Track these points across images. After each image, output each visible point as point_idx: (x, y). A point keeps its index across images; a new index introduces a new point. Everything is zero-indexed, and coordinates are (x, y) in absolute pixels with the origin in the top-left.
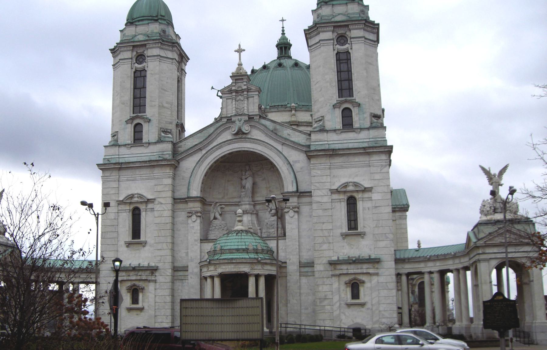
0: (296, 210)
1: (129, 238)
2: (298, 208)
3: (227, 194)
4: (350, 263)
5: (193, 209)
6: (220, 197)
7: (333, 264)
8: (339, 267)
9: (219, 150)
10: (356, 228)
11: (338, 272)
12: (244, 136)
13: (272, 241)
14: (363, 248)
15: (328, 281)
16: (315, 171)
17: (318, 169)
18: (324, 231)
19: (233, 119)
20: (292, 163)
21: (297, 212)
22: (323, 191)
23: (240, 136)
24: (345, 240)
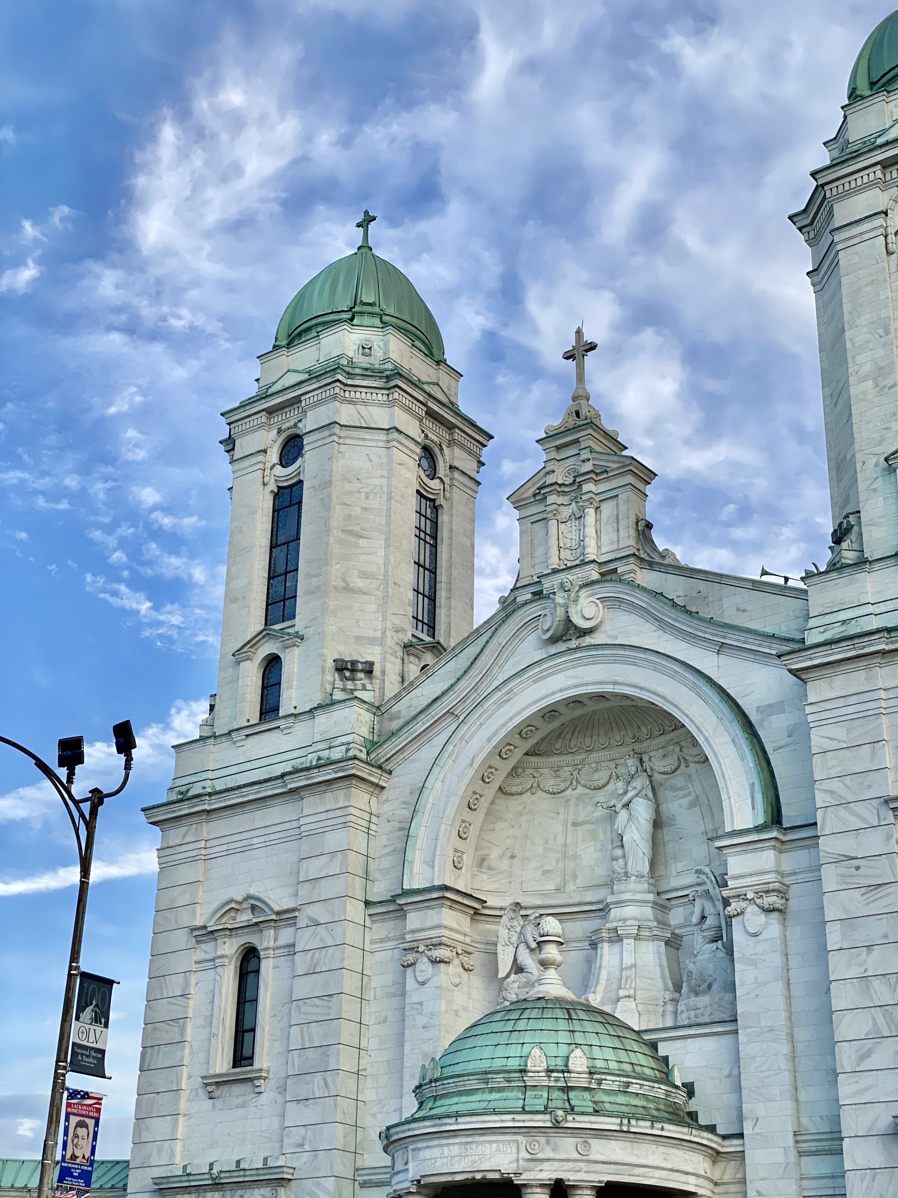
2: (782, 893)
3: (574, 876)
5: (422, 935)
6: (551, 886)
9: (507, 706)
12: (588, 640)
13: (692, 1045)
16: (823, 731)
17: (838, 721)
18: (876, 983)
19: (547, 584)
20: (754, 717)
22: (858, 808)
23: (573, 644)
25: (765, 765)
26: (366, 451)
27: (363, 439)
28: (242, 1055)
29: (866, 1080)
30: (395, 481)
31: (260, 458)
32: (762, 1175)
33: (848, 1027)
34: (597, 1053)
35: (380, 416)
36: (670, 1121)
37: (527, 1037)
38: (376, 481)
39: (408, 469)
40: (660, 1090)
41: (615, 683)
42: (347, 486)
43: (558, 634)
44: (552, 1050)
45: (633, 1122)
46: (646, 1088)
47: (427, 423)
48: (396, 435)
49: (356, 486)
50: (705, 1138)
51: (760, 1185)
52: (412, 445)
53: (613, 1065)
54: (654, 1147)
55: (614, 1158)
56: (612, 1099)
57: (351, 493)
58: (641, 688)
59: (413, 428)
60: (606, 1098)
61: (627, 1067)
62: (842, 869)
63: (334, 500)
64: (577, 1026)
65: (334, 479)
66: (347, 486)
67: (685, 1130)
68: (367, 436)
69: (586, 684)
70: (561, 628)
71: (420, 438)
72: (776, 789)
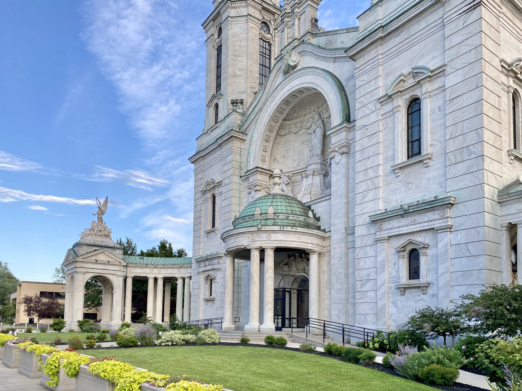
0: (344, 150)
1: (209, 227)
4: (402, 216)
7: (377, 221)
8: (387, 225)
10: (420, 153)
11: (384, 234)
14: (425, 184)
15: (370, 251)
21: (347, 153)
24: (400, 178)
25: (345, 100)
26: (240, 25)
27: (239, 21)
28: (214, 226)
29: (364, 206)
30: (249, 34)
31: (212, 37)
32: (335, 242)
33: (361, 188)
34: (279, 208)
35: (244, 11)
36: (299, 227)
37: (258, 205)
38: (243, 36)
39: (255, 30)
40: (302, 218)
41: (302, 84)
42: (234, 39)
43: (286, 71)
44: (264, 208)
45: (285, 227)
46: (295, 218)
47: (264, 13)
48: (249, 17)
49: (237, 38)
50: (320, 233)
51: (335, 246)
52: (256, 21)
53: (284, 211)
54: (294, 235)
55: (279, 239)
56: (282, 221)
57: (235, 41)
58: (309, 83)
59: (257, 15)
60: (280, 221)
61: (290, 212)
62: (362, 131)
63: (230, 44)
64: (275, 200)
65: (229, 37)
66: (234, 39)
67: (306, 229)
68: (240, 20)
69: (294, 87)
70: (287, 68)
71: (260, 17)
72: (349, 109)
